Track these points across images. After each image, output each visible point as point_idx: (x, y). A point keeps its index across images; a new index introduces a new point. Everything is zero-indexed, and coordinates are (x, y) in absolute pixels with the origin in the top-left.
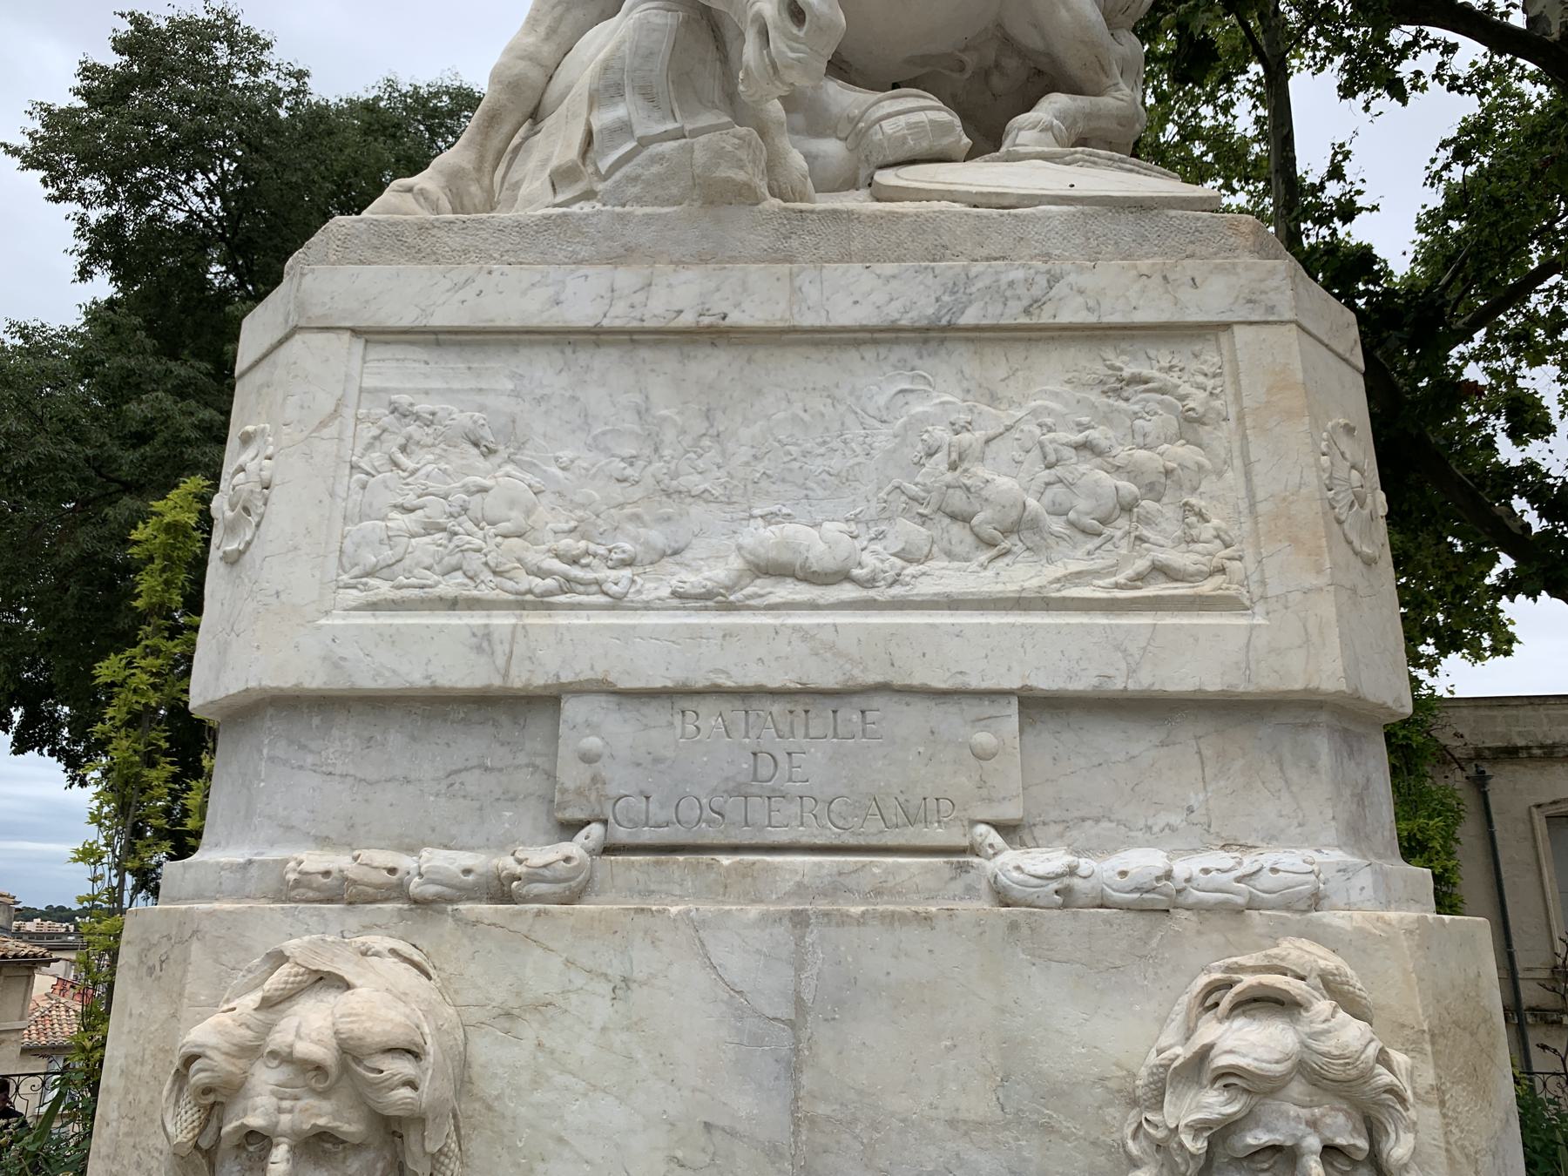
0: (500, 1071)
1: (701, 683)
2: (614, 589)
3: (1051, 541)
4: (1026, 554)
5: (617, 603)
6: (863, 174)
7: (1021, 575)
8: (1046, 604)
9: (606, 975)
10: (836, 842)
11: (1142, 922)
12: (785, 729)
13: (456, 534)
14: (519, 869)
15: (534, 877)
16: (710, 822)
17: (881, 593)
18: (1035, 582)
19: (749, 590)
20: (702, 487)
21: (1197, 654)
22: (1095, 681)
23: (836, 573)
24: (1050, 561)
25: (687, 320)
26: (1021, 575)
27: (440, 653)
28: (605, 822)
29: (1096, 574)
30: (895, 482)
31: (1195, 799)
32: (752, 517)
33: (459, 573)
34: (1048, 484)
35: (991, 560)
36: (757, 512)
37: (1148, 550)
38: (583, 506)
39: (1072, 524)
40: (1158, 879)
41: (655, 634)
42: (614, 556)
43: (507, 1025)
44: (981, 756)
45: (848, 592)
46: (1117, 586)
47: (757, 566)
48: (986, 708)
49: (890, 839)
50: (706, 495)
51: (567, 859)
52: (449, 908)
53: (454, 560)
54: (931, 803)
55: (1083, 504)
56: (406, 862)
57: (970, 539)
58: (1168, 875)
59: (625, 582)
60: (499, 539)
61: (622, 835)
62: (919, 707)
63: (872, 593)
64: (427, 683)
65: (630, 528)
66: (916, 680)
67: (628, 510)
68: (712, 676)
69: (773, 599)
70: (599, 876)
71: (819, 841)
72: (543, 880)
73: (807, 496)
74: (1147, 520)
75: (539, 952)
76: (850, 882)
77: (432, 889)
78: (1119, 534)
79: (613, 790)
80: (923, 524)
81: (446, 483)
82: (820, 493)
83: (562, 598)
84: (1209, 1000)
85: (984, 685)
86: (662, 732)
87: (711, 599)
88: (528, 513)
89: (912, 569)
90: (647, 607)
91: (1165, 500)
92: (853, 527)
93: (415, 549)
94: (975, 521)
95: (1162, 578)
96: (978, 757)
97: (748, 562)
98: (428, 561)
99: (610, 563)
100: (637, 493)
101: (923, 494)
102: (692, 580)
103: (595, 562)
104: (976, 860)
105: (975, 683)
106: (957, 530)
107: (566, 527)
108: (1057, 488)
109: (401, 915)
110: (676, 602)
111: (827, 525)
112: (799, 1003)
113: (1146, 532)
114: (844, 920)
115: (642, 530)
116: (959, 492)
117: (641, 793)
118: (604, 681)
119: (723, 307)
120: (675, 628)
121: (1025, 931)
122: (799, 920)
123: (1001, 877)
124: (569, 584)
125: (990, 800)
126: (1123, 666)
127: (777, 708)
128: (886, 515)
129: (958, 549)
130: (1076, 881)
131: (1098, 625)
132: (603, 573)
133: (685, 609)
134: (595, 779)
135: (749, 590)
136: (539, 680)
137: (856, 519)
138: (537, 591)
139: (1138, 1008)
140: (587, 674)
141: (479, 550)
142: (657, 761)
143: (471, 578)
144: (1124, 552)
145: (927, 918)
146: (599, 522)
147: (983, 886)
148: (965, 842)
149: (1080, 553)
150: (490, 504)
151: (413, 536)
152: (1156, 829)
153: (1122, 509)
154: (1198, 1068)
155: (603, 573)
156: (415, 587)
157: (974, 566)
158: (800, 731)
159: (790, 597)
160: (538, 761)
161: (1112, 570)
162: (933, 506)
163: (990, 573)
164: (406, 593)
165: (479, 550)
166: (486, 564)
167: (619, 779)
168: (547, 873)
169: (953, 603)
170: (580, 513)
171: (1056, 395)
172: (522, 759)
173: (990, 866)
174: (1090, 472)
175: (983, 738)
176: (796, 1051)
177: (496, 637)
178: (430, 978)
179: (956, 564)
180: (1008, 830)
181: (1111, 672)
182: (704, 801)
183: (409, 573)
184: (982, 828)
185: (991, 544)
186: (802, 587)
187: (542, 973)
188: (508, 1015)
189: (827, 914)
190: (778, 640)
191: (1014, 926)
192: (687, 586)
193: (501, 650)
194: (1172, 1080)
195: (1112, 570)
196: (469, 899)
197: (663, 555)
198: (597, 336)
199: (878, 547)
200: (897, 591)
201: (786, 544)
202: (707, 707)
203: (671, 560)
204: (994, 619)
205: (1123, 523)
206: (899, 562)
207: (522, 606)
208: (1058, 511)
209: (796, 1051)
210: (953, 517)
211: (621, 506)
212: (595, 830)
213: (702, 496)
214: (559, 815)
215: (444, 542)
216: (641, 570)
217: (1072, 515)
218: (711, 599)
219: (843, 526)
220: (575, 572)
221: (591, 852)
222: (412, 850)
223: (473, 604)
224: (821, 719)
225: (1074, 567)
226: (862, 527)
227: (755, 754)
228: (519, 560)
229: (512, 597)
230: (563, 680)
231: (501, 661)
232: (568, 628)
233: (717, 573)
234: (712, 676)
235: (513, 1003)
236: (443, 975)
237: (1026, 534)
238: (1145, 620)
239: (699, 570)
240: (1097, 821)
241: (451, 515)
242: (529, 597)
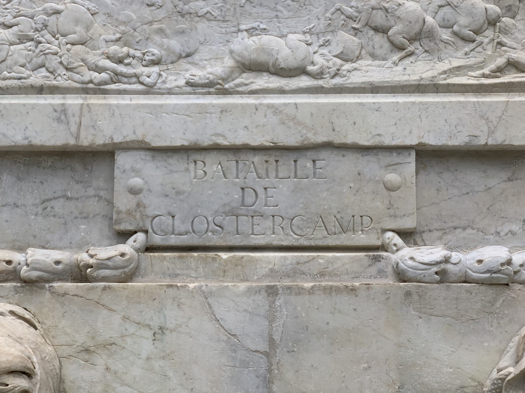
0: (83, 385)
1: (206, 142)
2: (147, 80)
3: (441, 45)
4: (424, 55)
5: (150, 90)
7: (420, 69)
8: (436, 88)
9: (149, 326)
10: (296, 244)
11: (490, 292)
12: (262, 172)
13: (40, 43)
14: (92, 261)
15: (101, 265)
16: (213, 232)
17: (327, 82)
18: (429, 74)
19: (238, 81)
20: (205, 10)
22: (467, 139)
23: (296, 69)
24: (440, 59)
26: (420, 69)
28: (146, 232)
29: (470, 68)
30: (338, 5)
32: (239, 31)
33: (43, 69)
34: (440, 7)
35: (401, 59)
36: (243, 27)
37: (506, 51)
38: (124, 23)
39: (455, 34)
40: (502, 265)
41: (175, 110)
42: (147, 58)
43: (87, 357)
44: (390, 188)
45: (304, 82)
46: (484, 76)
47: (243, 65)
48: (395, 158)
49: (331, 241)
50: (208, 15)
51: (123, 255)
52: (47, 285)
53: (40, 60)
54: (358, 219)
55: (463, 20)
56: (17, 257)
57: (387, 45)
58: (509, 262)
59: (154, 76)
60: (69, 46)
61: (157, 240)
62: (351, 158)
63: (321, 82)
64: (26, 142)
65: (157, 38)
66: (349, 140)
67: (156, 26)
68: (214, 138)
69: (254, 87)
70: (143, 265)
71: (285, 243)
72: (107, 267)
73: (277, 16)
74: (505, 31)
75: (105, 312)
76: (303, 268)
77: (35, 274)
78: (486, 40)
79: (150, 211)
80: (356, 35)
81: (32, 8)
82: (286, 13)
83: (113, 86)
85: (394, 143)
86: (180, 174)
87: (212, 87)
88: (88, 28)
89: (347, 66)
90: (170, 92)
91: (518, 17)
92: (308, 37)
93: (13, 53)
94: (390, 33)
95: (514, 70)
96: (389, 189)
97: (237, 62)
98: (22, 61)
99: (144, 63)
100: (161, 14)
101: (356, 14)
102: (199, 74)
103: (134, 62)
104: (385, 254)
105: (388, 141)
106: (378, 39)
107: (114, 37)
108: (447, 9)
109: (16, 290)
110: (189, 89)
111: (290, 36)
112: (271, 342)
113: (505, 40)
114: (300, 291)
115: (165, 40)
116: (381, 13)
117: (169, 214)
118: (142, 142)
120: (189, 106)
121: (415, 297)
122: (272, 292)
123: (401, 265)
124: (117, 77)
125: (395, 216)
126: (486, 129)
127: (257, 159)
128: (331, 28)
129: (378, 52)
130: (449, 267)
131: (470, 102)
132: (140, 70)
133: (195, 93)
134: (138, 205)
135: (238, 81)
136: (100, 141)
137: (310, 32)
138: (96, 81)
139: (486, 344)
140: (131, 137)
141: (56, 54)
142: (179, 193)
143: (51, 72)
144: (489, 53)
145: (353, 290)
146: (136, 34)
147: (390, 270)
148: (379, 243)
149: (460, 54)
150: (62, 22)
151: (11, 44)
152: (502, 234)
153: (489, 23)
155: (140, 70)
156: (14, 79)
157: (389, 63)
158: (273, 174)
159: (266, 85)
160: (102, 193)
161: (480, 66)
162: (363, 22)
163: (400, 68)
164: (9, 82)
165: (56, 54)
166: (61, 63)
167: (155, 205)
168: (110, 263)
169: (374, 89)
170: (122, 28)
172: (91, 192)
173: (394, 257)
175: (392, 177)
176: (270, 370)
177: (70, 112)
178: (36, 328)
179: (377, 62)
180: (407, 235)
181: (478, 133)
182: (210, 219)
183: (10, 69)
184: (390, 234)
185: (401, 48)
186: (274, 78)
187: (108, 325)
188: (87, 351)
189: (289, 288)
190: (260, 114)
191: (408, 294)
192: (196, 78)
193: (74, 121)
194: (506, 387)
195: (480, 66)
196: (60, 280)
197: (180, 57)
199: (325, 51)
200: (338, 81)
201: (262, 49)
202: (211, 159)
203: (185, 60)
204: (401, 99)
205: (489, 33)
206: (339, 61)
207: (86, 91)
208: (447, 25)
209: (270, 370)
210: (376, 30)
211: (151, 23)
212: (140, 237)
213: (206, 16)
214: (117, 227)
215: (33, 48)
216: (165, 67)
217: (455, 28)
218: (212, 87)
219: (301, 37)
220: (121, 68)
221: (138, 250)
222: (21, 249)
223: (54, 90)
224: (286, 165)
225: (456, 63)
226: (314, 37)
227: (243, 189)
228: (83, 60)
229: (79, 86)
230: (116, 141)
231: (74, 128)
232: (118, 106)
233: (216, 69)
234: (214, 138)
235: (90, 343)
236: (44, 327)
237: (425, 41)
239: (204, 67)
240: (464, 229)
241: (36, 30)
242: (91, 86)
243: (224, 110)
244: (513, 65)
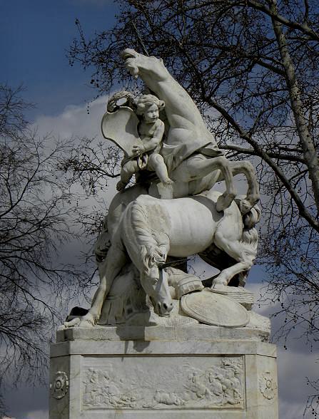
7: (204, 403)
26: (204, 403)
45: (174, 406)
169: (192, 409)
171: (212, 368)
223: (107, 409)
244: (229, 403)
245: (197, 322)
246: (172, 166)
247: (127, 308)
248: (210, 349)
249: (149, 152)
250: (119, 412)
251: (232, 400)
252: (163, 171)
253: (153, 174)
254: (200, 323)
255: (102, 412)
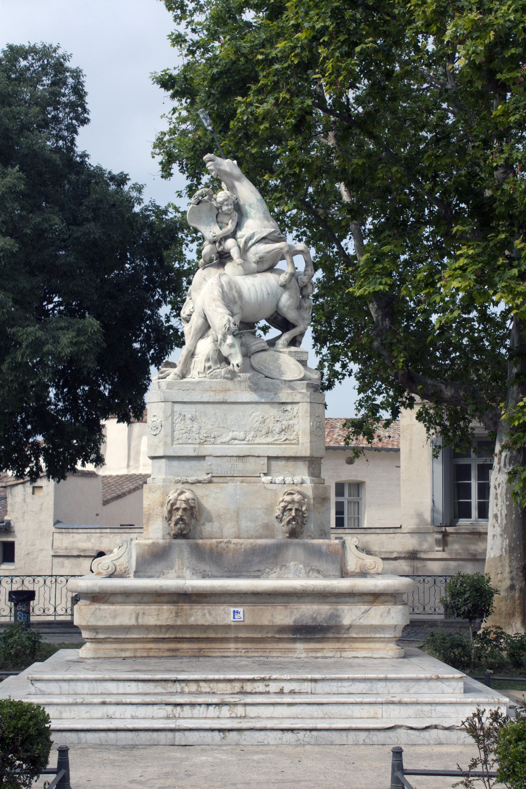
5: (213, 444)
6: (249, 355)
8: (272, 444)
21: (291, 451)
25: (221, 400)
26: (270, 440)
27: (189, 450)
31: (290, 470)
84: (284, 494)
100: (214, 427)
119: (226, 398)
136: (202, 455)
154: (283, 501)
174: (279, 425)
198: (208, 403)
204: (265, 446)
238: (284, 446)
243: (228, 448)
245: (263, 376)
246: (244, 248)
247: (208, 365)
248: (273, 398)
249: (225, 238)
250: (202, 446)
251: (289, 437)
252: (235, 253)
253: (227, 255)
254: (266, 377)
255: (188, 446)
